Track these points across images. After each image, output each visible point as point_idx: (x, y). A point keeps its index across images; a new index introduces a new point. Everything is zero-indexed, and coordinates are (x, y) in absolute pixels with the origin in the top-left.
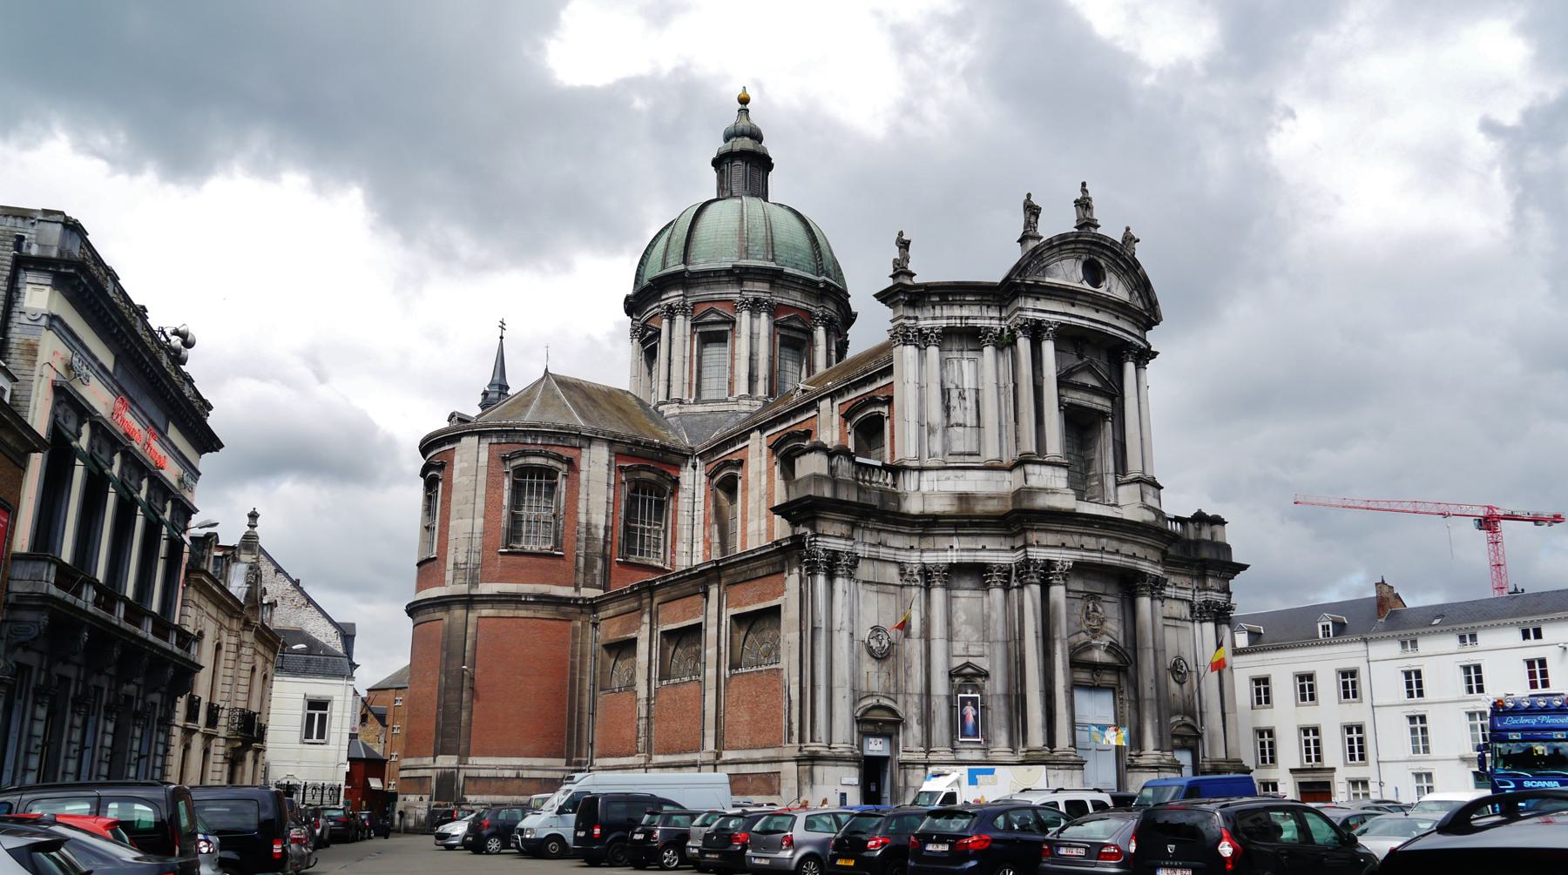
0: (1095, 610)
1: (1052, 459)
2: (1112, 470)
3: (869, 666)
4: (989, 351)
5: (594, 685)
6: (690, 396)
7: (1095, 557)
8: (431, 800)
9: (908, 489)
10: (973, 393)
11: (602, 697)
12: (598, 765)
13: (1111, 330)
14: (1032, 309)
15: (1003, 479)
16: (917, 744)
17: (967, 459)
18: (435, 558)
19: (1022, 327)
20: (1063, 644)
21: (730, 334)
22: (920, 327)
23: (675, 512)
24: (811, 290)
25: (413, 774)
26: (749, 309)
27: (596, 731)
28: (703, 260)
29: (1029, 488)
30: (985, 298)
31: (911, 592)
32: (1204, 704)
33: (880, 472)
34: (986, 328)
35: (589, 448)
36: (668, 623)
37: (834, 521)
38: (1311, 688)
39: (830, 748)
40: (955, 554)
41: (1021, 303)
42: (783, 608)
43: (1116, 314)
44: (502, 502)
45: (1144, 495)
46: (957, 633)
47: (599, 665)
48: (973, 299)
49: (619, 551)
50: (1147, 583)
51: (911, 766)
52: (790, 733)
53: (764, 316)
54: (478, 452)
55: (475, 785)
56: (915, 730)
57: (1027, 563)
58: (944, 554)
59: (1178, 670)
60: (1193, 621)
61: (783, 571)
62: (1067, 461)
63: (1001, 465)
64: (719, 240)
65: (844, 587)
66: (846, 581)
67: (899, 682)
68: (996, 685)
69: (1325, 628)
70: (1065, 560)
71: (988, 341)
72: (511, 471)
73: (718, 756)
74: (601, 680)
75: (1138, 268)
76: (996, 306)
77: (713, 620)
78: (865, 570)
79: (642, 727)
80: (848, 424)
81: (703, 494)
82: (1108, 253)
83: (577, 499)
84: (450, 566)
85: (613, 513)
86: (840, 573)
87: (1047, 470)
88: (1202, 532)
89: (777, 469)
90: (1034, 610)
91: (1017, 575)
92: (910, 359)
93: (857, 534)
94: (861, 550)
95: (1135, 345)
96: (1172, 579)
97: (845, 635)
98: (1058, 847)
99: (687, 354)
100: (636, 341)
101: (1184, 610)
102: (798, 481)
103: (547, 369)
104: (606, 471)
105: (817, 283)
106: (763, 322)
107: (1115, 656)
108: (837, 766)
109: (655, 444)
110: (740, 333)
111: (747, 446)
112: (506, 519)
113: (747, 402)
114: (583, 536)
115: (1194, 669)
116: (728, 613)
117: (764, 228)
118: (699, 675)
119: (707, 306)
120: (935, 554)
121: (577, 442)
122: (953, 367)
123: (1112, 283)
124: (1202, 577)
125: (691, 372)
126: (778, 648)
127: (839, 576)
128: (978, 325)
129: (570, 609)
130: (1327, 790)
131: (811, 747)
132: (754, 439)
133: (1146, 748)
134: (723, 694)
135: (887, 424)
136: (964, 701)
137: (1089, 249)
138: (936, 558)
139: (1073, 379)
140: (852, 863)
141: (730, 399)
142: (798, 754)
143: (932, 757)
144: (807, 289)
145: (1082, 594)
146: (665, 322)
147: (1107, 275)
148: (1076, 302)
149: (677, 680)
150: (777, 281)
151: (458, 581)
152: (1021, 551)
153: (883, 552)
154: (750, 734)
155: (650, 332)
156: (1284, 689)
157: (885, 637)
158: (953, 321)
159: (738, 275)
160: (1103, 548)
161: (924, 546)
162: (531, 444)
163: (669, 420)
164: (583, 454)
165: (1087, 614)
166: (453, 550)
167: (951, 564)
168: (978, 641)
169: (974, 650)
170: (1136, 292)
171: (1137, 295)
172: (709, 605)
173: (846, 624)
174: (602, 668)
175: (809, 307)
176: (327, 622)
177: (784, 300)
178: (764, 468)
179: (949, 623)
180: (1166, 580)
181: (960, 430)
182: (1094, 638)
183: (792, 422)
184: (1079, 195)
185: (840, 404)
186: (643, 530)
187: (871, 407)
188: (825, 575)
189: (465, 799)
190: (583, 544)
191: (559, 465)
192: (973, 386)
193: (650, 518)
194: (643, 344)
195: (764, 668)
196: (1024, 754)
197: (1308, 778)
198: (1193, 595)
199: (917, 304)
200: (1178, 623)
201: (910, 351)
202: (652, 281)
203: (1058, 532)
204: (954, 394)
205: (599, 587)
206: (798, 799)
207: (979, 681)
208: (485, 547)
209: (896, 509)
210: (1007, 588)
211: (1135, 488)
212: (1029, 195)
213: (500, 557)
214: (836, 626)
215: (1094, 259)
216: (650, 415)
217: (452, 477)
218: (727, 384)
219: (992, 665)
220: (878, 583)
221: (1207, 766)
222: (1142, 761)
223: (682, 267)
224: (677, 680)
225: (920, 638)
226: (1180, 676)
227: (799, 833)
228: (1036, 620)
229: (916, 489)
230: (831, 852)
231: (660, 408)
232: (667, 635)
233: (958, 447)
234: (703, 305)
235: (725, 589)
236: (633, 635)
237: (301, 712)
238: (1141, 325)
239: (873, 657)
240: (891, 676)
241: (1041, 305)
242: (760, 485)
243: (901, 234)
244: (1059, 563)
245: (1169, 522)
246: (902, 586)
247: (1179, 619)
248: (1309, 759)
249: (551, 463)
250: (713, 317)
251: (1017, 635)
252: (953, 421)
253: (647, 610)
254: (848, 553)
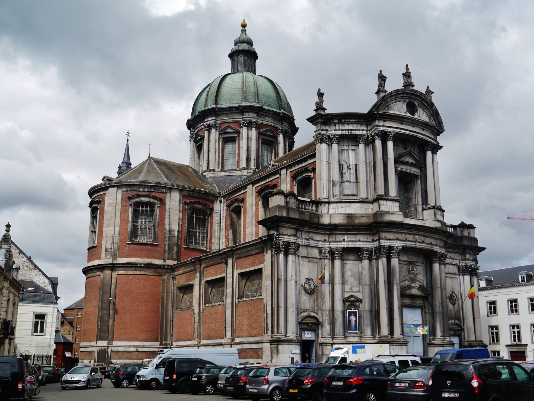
0: (413, 270)
1: (392, 198)
2: (420, 202)
3: (305, 297)
4: (362, 146)
5: (173, 307)
6: (218, 168)
7: (413, 244)
8: (95, 362)
9: (323, 212)
10: (354, 166)
11: (176, 312)
12: (175, 345)
13: (420, 136)
14: (382, 126)
15: (368, 207)
16: (328, 334)
17: (351, 197)
18: (96, 246)
19: (377, 135)
20: (397, 285)
21: (237, 138)
22: (328, 134)
23: (212, 224)
24: (276, 117)
25: (86, 349)
26: (247, 126)
27: (174, 329)
28: (225, 102)
29: (381, 212)
30: (360, 121)
31: (324, 262)
32: (465, 314)
33: (310, 204)
34: (361, 135)
35: (170, 193)
36: (208, 277)
37: (288, 228)
38: (516, 306)
39: (286, 336)
40: (345, 243)
41: (377, 123)
42: (263, 269)
43: (423, 128)
44: (128, 219)
45: (436, 214)
46: (346, 281)
47: (175, 297)
48: (354, 121)
49: (185, 242)
50: (437, 257)
51: (325, 345)
52: (267, 329)
53: (254, 129)
54: (117, 195)
55: (116, 355)
56: (327, 327)
57: (380, 247)
58: (341, 243)
59: (453, 298)
60: (459, 275)
61: (263, 252)
62: (399, 199)
63: (368, 200)
64: (232, 93)
65: (292, 259)
66: (294, 256)
67: (319, 305)
68: (366, 306)
69: (522, 278)
70: (398, 246)
71: (361, 141)
72: (133, 204)
73: (233, 340)
74: (176, 304)
75: (433, 106)
76: (365, 124)
77: (230, 275)
78: (303, 251)
79: (196, 327)
80: (294, 181)
81: (225, 215)
82: (419, 99)
83: (165, 218)
84: (103, 250)
85: (182, 224)
86: (291, 252)
87: (389, 203)
88: (464, 232)
89: (260, 203)
90: (384, 270)
91: (375, 253)
92: (324, 150)
93: (299, 234)
94: (301, 242)
95: (431, 143)
96: (450, 255)
97: (293, 282)
98: (395, 383)
99: (217, 148)
100: (192, 141)
101: (455, 270)
102: (270, 209)
103: (149, 156)
104: (178, 204)
105: (279, 113)
106: (254, 132)
107: (422, 292)
108: (289, 345)
109: (202, 191)
110: (242, 138)
111: (246, 192)
112: (130, 227)
113: (246, 171)
114: (167, 235)
115: (460, 297)
116: (237, 272)
117: (254, 87)
118: (223, 302)
119: (227, 125)
120: (336, 243)
121: (164, 190)
122: (345, 154)
123: (421, 113)
124: (464, 254)
125: (219, 156)
126: (261, 288)
127: (290, 254)
128: (357, 134)
129: (161, 270)
130: (523, 355)
131: (277, 336)
132: (249, 189)
133: (437, 336)
134: (235, 311)
135: (313, 181)
136: (350, 314)
137: (410, 97)
138: (336, 245)
139: (402, 159)
140: (296, 391)
141: (238, 169)
142: (271, 339)
143: (335, 340)
144: (274, 117)
145: (406, 262)
146: (206, 132)
147: (418, 109)
148: (403, 122)
149: (213, 304)
150: (260, 113)
151: (107, 257)
152: (377, 242)
153: (311, 243)
154: (247, 330)
155: (199, 137)
156: (503, 307)
157: (313, 283)
158: (344, 132)
159: (241, 110)
160: (416, 240)
161: (330, 240)
162: (142, 191)
163: (209, 179)
164: (167, 196)
165: (409, 271)
166: (105, 242)
167: (344, 248)
168: (357, 285)
169: (355, 289)
170: (432, 118)
171: (432, 119)
172: (228, 268)
173: (294, 277)
174: (177, 299)
175: (275, 125)
176: (44, 277)
177: (263, 122)
178: (254, 202)
179: (343, 276)
180: (447, 255)
181: (348, 184)
182: (412, 283)
183: (267, 181)
184: (405, 71)
185: (290, 172)
186: (196, 232)
187: (305, 173)
188: (284, 254)
189: (111, 362)
190: (167, 239)
191: (156, 201)
192: (354, 163)
193: (199, 226)
194: (196, 143)
195: (254, 298)
196: (379, 339)
197: (515, 349)
198: (460, 262)
199: (327, 124)
200: (452, 276)
201: (324, 146)
202: (200, 112)
203: (394, 232)
204: (345, 166)
205: (175, 260)
206: (271, 360)
207: (357, 304)
208: (120, 241)
209: (317, 222)
210: (370, 260)
211: (432, 211)
212: (381, 71)
213: (127, 245)
214: (289, 278)
215: (412, 102)
216: (200, 178)
217: (104, 207)
218: (236, 162)
219: (364, 296)
220: (309, 257)
221: (466, 344)
222: (435, 342)
223: (214, 106)
224: (213, 304)
225: (329, 283)
226: (453, 301)
227: (271, 376)
228: (384, 274)
229: (327, 212)
230: (286, 386)
231: (204, 174)
232: (207, 282)
233: (347, 192)
234: (224, 124)
235: (236, 261)
236: (192, 283)
237: (32, 320)
238: (434, 133)
239: (307, 292)
240: (315, 302)
241: (387, 124)
242: (252, 211)
243: (319, 90)
244: (395, 248)
245: (448, 228)
246: (320, 259)
247: (453, 274)
248: (515, 340)
249: (152, 200)
250: (229, 130)
251: (376, 282)
252: (344, 180)
253: (198, 270)
254: (294, 243)
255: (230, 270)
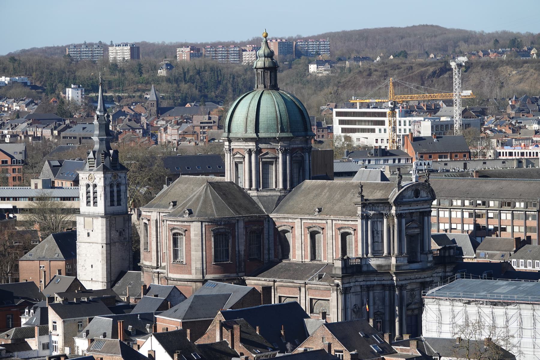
2: (419, 251)
10: (381, 232)
23: (263, 238)
36: (282, 294)
42: (330, 301)
64: (268, 122)
78: (353, 290)
101: (439, 279)
114: (237, 255)
181: (377, 243)
204: (375, 232)
210: (390, 290)
241: (401, 208)
255: (303, 295)
